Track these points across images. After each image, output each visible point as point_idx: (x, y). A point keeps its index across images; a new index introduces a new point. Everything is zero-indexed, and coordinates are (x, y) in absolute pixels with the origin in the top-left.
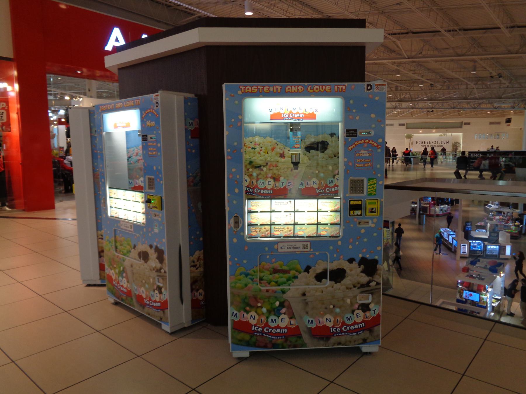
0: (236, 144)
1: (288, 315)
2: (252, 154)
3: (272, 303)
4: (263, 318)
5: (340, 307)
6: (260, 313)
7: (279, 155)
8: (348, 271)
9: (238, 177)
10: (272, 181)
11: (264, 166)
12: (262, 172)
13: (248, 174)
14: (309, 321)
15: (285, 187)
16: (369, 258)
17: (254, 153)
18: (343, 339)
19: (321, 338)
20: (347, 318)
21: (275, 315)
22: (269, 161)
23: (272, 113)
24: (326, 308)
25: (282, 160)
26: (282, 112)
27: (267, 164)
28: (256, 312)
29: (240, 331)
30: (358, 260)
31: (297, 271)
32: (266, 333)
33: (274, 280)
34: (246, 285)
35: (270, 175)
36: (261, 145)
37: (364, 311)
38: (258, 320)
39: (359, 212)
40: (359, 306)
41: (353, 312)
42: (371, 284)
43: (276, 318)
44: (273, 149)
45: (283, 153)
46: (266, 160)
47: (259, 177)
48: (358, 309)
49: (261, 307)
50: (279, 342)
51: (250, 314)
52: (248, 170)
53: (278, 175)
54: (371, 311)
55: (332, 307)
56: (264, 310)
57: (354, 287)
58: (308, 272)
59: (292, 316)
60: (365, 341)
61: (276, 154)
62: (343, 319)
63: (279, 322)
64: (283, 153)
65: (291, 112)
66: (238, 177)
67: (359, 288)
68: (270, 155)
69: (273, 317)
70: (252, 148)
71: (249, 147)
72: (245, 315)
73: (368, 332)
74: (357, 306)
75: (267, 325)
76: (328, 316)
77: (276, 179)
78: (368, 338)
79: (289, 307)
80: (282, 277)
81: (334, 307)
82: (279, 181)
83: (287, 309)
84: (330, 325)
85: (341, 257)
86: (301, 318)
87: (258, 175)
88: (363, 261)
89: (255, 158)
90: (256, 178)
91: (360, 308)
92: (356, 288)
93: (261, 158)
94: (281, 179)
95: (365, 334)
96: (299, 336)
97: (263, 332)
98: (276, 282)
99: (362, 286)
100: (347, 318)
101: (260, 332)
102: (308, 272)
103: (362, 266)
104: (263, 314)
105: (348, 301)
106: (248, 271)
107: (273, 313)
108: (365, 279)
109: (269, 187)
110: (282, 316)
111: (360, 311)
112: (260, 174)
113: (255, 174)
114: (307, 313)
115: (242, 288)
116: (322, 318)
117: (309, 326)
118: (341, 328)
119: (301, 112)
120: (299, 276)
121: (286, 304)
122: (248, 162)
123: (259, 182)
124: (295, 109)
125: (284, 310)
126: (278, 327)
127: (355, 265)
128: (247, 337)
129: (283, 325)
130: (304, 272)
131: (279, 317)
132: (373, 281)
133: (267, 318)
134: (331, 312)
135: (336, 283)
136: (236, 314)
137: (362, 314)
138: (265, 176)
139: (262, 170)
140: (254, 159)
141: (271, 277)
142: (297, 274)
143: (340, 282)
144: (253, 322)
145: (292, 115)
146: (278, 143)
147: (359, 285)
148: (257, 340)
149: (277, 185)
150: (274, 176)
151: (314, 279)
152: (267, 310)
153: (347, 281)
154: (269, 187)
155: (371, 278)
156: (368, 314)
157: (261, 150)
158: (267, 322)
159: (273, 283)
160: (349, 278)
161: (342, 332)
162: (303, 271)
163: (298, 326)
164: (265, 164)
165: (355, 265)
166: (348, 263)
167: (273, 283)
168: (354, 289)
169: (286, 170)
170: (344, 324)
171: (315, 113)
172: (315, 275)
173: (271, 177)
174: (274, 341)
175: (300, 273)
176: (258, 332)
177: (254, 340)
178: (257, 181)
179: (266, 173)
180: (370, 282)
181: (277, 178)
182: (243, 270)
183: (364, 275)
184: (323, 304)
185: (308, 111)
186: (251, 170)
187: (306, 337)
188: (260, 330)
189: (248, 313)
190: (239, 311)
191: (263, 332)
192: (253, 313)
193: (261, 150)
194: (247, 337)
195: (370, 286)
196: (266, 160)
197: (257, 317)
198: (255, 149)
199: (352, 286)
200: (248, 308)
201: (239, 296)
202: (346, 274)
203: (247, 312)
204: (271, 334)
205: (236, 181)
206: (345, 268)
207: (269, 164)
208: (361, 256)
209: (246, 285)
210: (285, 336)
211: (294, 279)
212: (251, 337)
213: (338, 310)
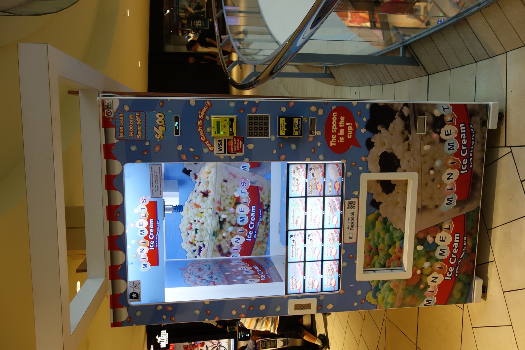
0: (197, 312)
1: (436, 232)
2: (204, 233)
3: (419, 256)
4: (437, 265)
5: (435, 160)
6: (430, 270)
7: (205, 198)
8: (384, 149)
9: (243, 306)
10: (239, 207)
11: (220, 217)
12: (227, 220)
13: (230, 237)
14: (447, 204)
15: (248, 190)
16: (369, 117)
17: (202, 230)
18: (477, 155)
19: (473, 186)
20: (449, 149)
21: (434, 250)
22: (213, 211)
23: (149, 264)
24: (433, 180)
25: (211, 195)
26: (146, 250)
27: (217, 213)
28: (428, 276)
29: (450, 295)
30: (369, 135)
31: (376, 219)
32: (457, 262)
33: (386, 250)
34: (391, 290)
35: (232, 210)
36: (192, 222)
37: (443, 124)
38: (439, 273)
39: (296, 121)
40: (436, 132)
41: (443, 141)
42: (406, 114)
43: (438, 249)
44: (197, 206)
45: (202, 192)
46: (211, 215)
47: (234, 223)
48: (439, 133)
49: (422, 269)
50: (470, 244)
51: (429, 283)
52: (224, 237)
53: (231, 199)
54: (444, 113)
55: (432, 172)
56: (427, 265)
57: (407, 139)
58: (380, 203)
59: (439, 228)
60: (484, 123)
61: (204, 202)
62: (451, 155)
63: (444, 245)
64: (202, 192)
65: (146, 238)
66: (243, 306)
67: (410, 133)
68: (204, 210)
69: (438, 252)
70: (196, 232)
71: (195, 237)
72: (430, 289)
73: (473, 118)
74: (435, 135)
75: (446, 261)
76: (445, 177)
77: (238, 201)
78: (481, 118)
79: (427, 231)
80: (383, 239)
81: (432, 169)
82: (239, 197)
83: (428, 234)
84: (456, 174)
85: (363, 159)
86: (442, 215)
87: (232, 225)
88: (372, 127)
89: (209, 229)
90: (235, 228)
91: (438, 130)
92: (409, 136)
93: (209, 222)
94: (237, 195)
95: (476, 126)
96: (466, 216)
97: (455, 266)
98: (390, 246)
99: (407, 127)
100: (449, 149)
101: (455, 270)
102: (380, 203)
103: (379, 128)
104: (431, 266)
105: (426, 148)
106: (373, 288)
107: (431, 254)
108: (397, 124)
109: (247, 210)
110: (437, 241)
111: (443, 130)
112: (229, 222)
113: (230, 229)
114: (437, 207)
115: (395, 294)
116: (446, 185)
117: (454, 203)
118: (462, 158)
119: (146, 224)
120: (384, 216)
121: (421, 236)
122: (214, 238)
123: (241, 224)
124: (142, 232)
125: (430, 239)
126: (451, 246)
127: (376, 139)
128: (459, 286)
129: (449, 239)
130: (378, 209)
131: (438, 245)
132: (401, 111)
133: (437, 260)
134: (439, 173)
135: (400, 166)
136: (427, 301)
137: (447, 128)
138: (233, 215)
139: (225, 219)
140: (210, 230)
141: (381, 254)
142: (380, 219)
143: (399, 161)
144: (441, 278)
145: (151, 236)
146: (189, 200)
147: (406, 132)
148: (464, 273)
149: (245, 200)
150: (233, 204)
151: (390, 195)
152: (427, 261)
153: (399, 151)
154: (247, 210)
155: (397, 114)
156: (449, 118)
157: (199, 221)
158: (442, 260)
159: (390, 251)
160: (394, 147)
161: (468, 157)
162: (377, 212)
163: (452, 219)
164: (217, 216)
165: (376, 139)
166: (373, 149)
167: (390, 251)
168: (410, 139)
169: (225, 189)
170: (457, 155)
171: (147, 203)
172: (384, 194)
173: (235, 208)
174: (469, 251)
175: (379, 215)
176: (454, 273)
177: (463, 277)
178: (239, 226)
179: (228, 214)
180: (402, 116)
181: (235, 199)
182: (370, 295)
183: (392, 125)
184: (426, 185)
185: (145, 212)
186: (224, 234)
187: (469, 208)
188: (451, 269)
189: (429, 286)
190: (425, 297)
191: (455, 266)
192: (430, 279)
193: (199, 221)
194: (459, 286)
195: (409, 116)
196: (211, 215)
197: (435, 274)
198: (196, 230)
199: (407, 142)
200: (422, 286)
201: (404, 299)
202: (389, 151)
203: (427, 286)
204: (458, 255)
205: (249, 309)
206: (380, 153)
207: (218, 211)
208: (363, 130)
209: (391, 290)
210: (464, 236)
211: (388, 223)
212: (459, 280)
213: (438, 163)
